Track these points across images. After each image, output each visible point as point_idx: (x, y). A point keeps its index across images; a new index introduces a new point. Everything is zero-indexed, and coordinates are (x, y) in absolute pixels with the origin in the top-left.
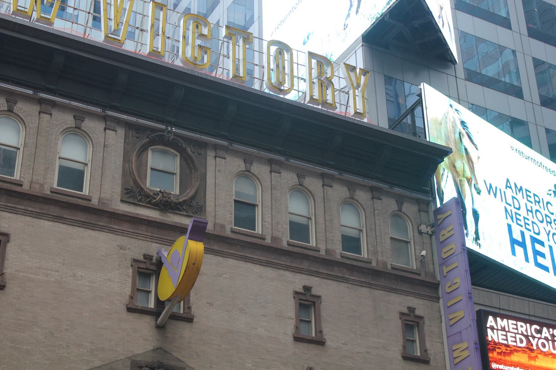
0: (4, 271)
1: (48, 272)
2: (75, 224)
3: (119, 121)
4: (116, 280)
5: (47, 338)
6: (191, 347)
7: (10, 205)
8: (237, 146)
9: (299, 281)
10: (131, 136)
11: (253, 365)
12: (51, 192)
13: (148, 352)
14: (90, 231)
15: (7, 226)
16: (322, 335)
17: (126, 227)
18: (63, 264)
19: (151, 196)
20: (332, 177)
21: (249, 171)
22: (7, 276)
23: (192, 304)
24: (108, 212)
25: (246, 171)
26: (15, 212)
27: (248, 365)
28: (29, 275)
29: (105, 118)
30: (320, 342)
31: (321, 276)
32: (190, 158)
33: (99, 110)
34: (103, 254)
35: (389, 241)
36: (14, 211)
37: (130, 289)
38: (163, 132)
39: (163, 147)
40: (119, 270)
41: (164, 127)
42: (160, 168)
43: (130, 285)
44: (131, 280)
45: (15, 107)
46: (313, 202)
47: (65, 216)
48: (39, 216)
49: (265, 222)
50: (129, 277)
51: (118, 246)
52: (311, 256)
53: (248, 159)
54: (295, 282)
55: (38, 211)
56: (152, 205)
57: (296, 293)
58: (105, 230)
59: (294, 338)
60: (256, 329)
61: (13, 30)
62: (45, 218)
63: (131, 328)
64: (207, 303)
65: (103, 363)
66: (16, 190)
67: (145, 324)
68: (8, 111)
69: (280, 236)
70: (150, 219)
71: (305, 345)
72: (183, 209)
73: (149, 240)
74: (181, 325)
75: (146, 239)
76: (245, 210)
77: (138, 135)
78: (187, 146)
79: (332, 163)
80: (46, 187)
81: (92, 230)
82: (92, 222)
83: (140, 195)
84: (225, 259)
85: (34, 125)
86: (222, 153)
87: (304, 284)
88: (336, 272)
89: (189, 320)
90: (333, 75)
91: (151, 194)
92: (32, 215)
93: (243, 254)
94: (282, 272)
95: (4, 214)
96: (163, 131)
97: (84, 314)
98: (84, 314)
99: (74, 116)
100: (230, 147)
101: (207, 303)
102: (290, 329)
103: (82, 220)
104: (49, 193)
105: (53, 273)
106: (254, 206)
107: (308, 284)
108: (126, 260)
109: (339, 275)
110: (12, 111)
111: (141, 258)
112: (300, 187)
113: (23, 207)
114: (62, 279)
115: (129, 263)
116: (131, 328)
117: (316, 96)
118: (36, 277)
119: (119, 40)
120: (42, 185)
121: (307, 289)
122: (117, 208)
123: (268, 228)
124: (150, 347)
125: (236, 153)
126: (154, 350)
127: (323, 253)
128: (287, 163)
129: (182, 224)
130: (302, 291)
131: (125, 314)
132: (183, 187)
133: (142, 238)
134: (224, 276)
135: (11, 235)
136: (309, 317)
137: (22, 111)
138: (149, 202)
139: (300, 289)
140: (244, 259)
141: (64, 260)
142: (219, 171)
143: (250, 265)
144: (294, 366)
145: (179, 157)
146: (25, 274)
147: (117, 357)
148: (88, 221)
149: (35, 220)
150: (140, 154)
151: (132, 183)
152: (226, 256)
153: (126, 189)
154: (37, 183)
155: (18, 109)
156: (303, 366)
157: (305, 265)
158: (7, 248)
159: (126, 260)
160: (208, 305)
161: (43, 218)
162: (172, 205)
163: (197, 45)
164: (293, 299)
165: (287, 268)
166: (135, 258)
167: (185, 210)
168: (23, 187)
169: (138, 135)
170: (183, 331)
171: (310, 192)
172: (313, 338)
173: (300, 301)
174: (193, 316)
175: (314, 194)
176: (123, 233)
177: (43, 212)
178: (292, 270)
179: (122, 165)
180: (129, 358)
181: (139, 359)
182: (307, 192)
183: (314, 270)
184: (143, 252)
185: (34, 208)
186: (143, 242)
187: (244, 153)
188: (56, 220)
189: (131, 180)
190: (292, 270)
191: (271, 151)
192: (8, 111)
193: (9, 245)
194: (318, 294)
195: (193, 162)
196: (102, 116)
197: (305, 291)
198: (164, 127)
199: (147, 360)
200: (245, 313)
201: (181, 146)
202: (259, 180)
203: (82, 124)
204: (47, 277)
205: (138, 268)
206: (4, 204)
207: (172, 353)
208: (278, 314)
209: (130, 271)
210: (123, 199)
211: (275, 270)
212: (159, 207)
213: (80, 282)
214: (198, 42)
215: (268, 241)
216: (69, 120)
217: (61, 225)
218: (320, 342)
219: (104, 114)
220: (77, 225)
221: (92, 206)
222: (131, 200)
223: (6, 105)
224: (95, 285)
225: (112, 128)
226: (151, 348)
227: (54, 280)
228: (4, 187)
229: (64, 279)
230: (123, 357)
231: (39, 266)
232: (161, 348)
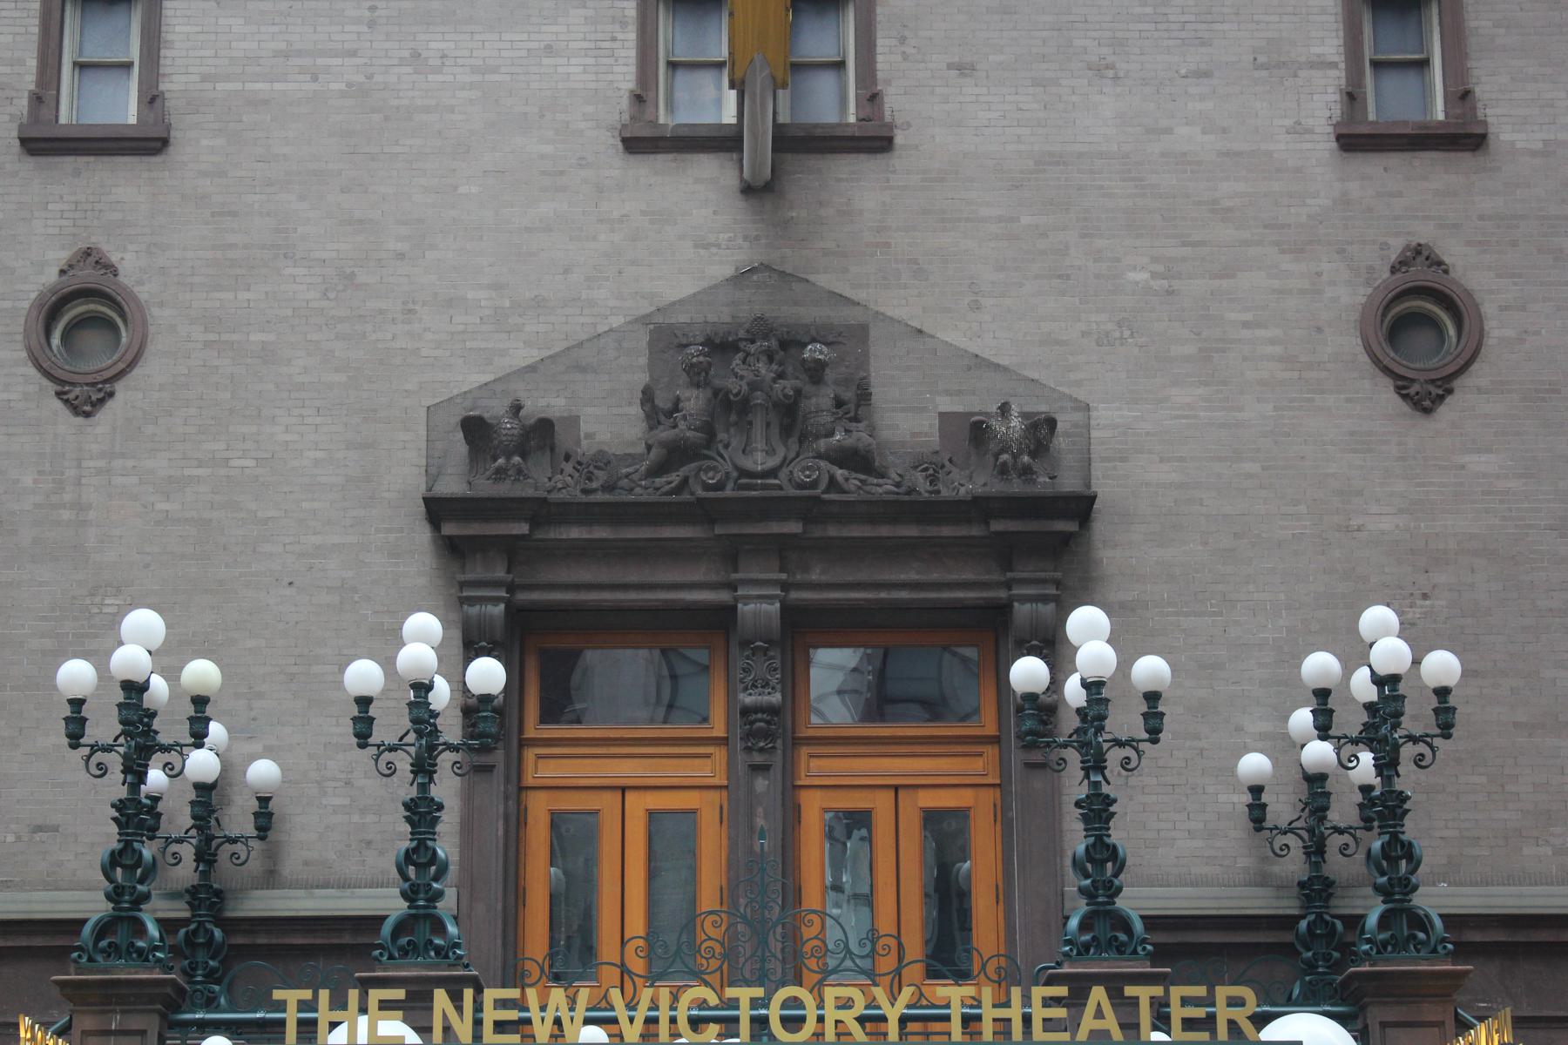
0: (162, 87)
1: (320, 61)
4: (573, 45)
5: (332, 295)
6: (888, 245)
11: (1154, 275)
13: (715, 287)
16: (1474, 108)
18: (372, 24)
22: (171, 104)
23: (888, 82)
27: (1132, 276)
28: (249, 86)
30: (1463, 138)
37: (633, 69)
43: (633, 53)
50: (624, 24)
59: (1339, 138)
60: (1168, 131)
63: (643, 213)
64: (950, 66)
65: (545, 353)
67: (702, 188)
71: (1395, 160)
74: (843, 166)
89: (874, 141)
97: (462, 190)
98: (462, 190)
101: (950, 66)
102: (1322, 105)
105: (339, 61)
114: (370, 77)
116: (643, 213)
118: (277, 86)
124: (722, 269)
126: (741, 278)
131: (617, 166)
136: (1422, 42)
141: (373, 9)
144: (1341, 252)
146: (237, 86)
147: (594, 325)
156: (1384, 246)
160: (954, 73)
170: (859, 187)
172: (1440, 122)
174: (891, 126)
180: (644, 320)
181: (683, 318)
199: (712, 318)
200: (1116, 78)
204: (315, 79)
207: (811, 278)
208: (1262, 59)
213: (439, 78)
218: (1463, 138)
224: (496, 77)
226: (729, 271)
227: (343, 86)
229: (379, 78)
230: (616, 321)
231: (283, 46)
232: (765, 267)
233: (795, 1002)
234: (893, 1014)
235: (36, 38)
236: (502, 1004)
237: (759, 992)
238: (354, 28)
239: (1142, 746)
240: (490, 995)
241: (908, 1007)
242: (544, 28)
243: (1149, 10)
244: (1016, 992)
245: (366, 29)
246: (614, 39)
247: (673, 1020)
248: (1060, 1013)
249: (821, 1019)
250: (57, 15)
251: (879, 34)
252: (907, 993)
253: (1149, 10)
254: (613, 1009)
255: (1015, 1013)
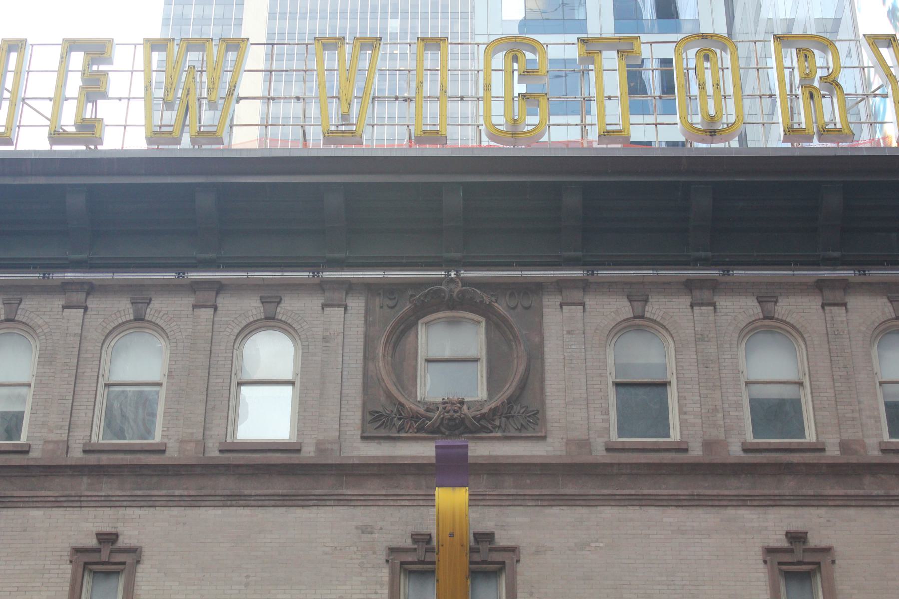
2: (266, 503)
3: (349, 287)
7: (139, 493)
8: (604, 273)
9: (773, 525)
10: (377, 309)
12: (221, 451)
14: (299, 512)
15: (137, 532)
17: (372, 487)
18: (247, 585)
19: (423, 416)
20: (845, 286)
21: (642, 317)
24: (331, 465)
25: (635, 318)
26: (151, 503)
29: (322, 286)
31: (830, 503)
32: (505, 320)
33: (303, 275)
34: (327, 549)
35: (612, 391)
36: (149, 502)
38: (440, 284)
39: (449, 314)
40: (361, 575)
41: (441, 274)
42: (447, 354)
44: (386, 591)
45: (148, 310)
46: (803, 347)
47: (246, 492)
48: (194, 501)
49: (685, 413)
51: (357, 528)
52: (798, 464)
53: (638, 294)
54: (766, 528)
55: (192, 493)
56: (428, 433)
57: (770, 551)
58: (328, 503)
61: (110, 174)
62: (208, 503)
66: (149, 462)
68: (137, 320)
69: (722, 437)
70: (419, 461)
72: (495, 427)
73: (421, 503)
75: (415, 503)
76: (643, 395)
77: (391, 303)
78: (494, 299)
79: (836, 254)
80: (210, 445)
81: (303, 506)
82: (301, 492)
83: (399, 419)
84: (594, 509)
85: (184, 334)
86: (577, 295)
87: (785, 529)
88: (870, 486)
90: (838, 68)
91: (421, 410)
92: (182, 503)
93: (633, 492)
94: (731, 512)
95: (130, 512)
96: (438, 281)
99: (261, 297)
100: (591, 279)
103: (280, 492)
104: (216, 454)
106: (664, 385)
107: (796, 525)
108: (374, 553)
109: (875, 493)
110: (143, 320)
111: (408, 542)
112: (767, 322)
113: (164, 492)
115: (382, 556)
117: (802, 120)
119: (352, 132)
120: (202, 444)
121: (797, 538)
122: (355, 453)
123: (694, 425)
125: (610, 287)
127: (833, 452)
128: (727, 279)
129: (497, 457)
130: (785, 544)
132: (494, 381)
133: (407, 503)
134: (593, 544)
135: (144, 549)
137: (161, 314)
138: (419, 430)
139: (778, 540)
140: (636, 502)
141: (247, 576)
142: (569, 333)
143: (653, 512)
145: (484, 324)
148: (292, 492)
149: (190, 512)
150: (399, 339)
151: (383, 399)
152: (596, 503)
153: (371, 413)
154: (191, 441)
155: (153, 312)
157: (789, 486)
158: (137, 574)
159: (374, 553)
161: (203, 503)
162: (467, 423)
163: (516, 95)
164: (762, 565)
165: (743, 501)
166: (394, 545)
167: (500, 427)
168: (167, 454)
169: (391, 303)
171: (793, 327)
173: (784, 567)
175: (801, 330)
176: (365, 501)
177: (203, 492)
178: (756, 503)
179: (361, 369)
182: (788, 329)
183: (811, 492)
184: (410, 529)
185: (187, 489)
186: (410, 510)
187: (626, 283)
188: (229, 503)
189: (382, 393)
190: (756, 503)
191: (818, 265)
192: (137, 320)
193: (140, 568)
194: (824, 544)
195: (511, 328)
196: (316, 284)
197: (791, 543)
198: (441, 274)
201: (482, 302)
202: (667, 330)
203: (278, 310)
205: (402, 563)
206: (129, 493)
209: (384, 573)
210: (365, 435)
211: (714, 510)
212: (443, 433)
214: (520, 88)
215: (696, 452)
216: (123, 307)
217: (241, 511)
219: (317, 280)
220: (272, 503)
221: (297, 462)
222: (383, 433)
223: (131, 311)
225: (335, 303)
228: (124, 463)
235: (67, 593)
238: (237, 587)
242: (339, 587)
243: (664, 578)
245: (243, 587)
246: (376, 593)
250: (80, 580)
251: (519, 591)
253: (664, 578)
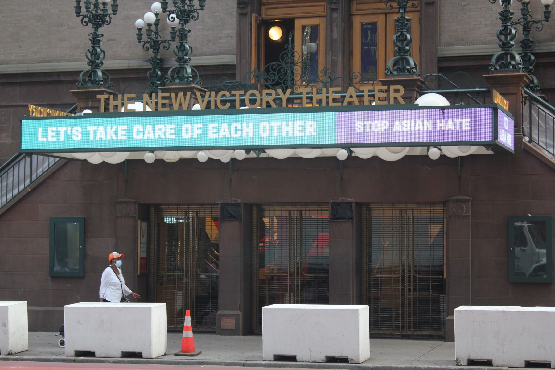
233: (253, 95)
234: (284, 98)
236: (163, 98)
237: (242, 92)
239: (198, 11)
240: (161, 95)
241: (250, 96)
244: (324, 90)
247: (216, 101)
248: (338, 96)
249: (261, 99)
252: (289, 91)
254: (279, 95)
255: (323, 96)
